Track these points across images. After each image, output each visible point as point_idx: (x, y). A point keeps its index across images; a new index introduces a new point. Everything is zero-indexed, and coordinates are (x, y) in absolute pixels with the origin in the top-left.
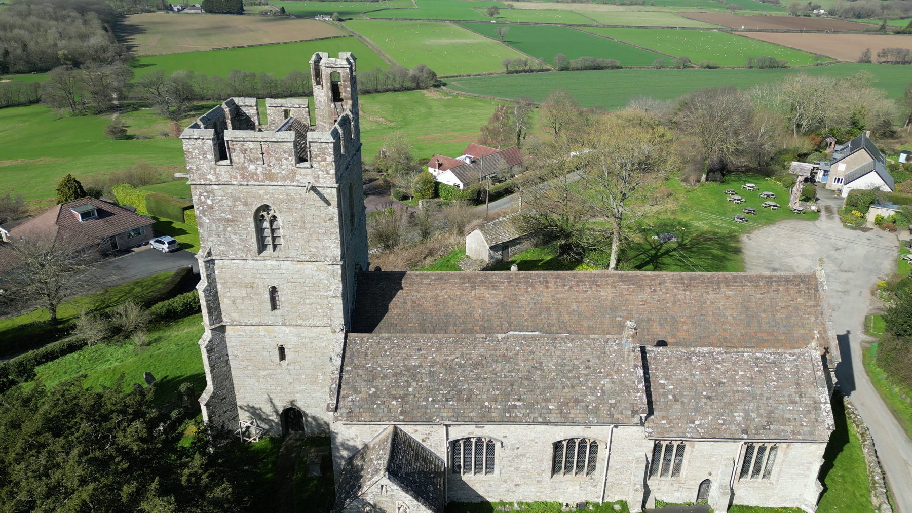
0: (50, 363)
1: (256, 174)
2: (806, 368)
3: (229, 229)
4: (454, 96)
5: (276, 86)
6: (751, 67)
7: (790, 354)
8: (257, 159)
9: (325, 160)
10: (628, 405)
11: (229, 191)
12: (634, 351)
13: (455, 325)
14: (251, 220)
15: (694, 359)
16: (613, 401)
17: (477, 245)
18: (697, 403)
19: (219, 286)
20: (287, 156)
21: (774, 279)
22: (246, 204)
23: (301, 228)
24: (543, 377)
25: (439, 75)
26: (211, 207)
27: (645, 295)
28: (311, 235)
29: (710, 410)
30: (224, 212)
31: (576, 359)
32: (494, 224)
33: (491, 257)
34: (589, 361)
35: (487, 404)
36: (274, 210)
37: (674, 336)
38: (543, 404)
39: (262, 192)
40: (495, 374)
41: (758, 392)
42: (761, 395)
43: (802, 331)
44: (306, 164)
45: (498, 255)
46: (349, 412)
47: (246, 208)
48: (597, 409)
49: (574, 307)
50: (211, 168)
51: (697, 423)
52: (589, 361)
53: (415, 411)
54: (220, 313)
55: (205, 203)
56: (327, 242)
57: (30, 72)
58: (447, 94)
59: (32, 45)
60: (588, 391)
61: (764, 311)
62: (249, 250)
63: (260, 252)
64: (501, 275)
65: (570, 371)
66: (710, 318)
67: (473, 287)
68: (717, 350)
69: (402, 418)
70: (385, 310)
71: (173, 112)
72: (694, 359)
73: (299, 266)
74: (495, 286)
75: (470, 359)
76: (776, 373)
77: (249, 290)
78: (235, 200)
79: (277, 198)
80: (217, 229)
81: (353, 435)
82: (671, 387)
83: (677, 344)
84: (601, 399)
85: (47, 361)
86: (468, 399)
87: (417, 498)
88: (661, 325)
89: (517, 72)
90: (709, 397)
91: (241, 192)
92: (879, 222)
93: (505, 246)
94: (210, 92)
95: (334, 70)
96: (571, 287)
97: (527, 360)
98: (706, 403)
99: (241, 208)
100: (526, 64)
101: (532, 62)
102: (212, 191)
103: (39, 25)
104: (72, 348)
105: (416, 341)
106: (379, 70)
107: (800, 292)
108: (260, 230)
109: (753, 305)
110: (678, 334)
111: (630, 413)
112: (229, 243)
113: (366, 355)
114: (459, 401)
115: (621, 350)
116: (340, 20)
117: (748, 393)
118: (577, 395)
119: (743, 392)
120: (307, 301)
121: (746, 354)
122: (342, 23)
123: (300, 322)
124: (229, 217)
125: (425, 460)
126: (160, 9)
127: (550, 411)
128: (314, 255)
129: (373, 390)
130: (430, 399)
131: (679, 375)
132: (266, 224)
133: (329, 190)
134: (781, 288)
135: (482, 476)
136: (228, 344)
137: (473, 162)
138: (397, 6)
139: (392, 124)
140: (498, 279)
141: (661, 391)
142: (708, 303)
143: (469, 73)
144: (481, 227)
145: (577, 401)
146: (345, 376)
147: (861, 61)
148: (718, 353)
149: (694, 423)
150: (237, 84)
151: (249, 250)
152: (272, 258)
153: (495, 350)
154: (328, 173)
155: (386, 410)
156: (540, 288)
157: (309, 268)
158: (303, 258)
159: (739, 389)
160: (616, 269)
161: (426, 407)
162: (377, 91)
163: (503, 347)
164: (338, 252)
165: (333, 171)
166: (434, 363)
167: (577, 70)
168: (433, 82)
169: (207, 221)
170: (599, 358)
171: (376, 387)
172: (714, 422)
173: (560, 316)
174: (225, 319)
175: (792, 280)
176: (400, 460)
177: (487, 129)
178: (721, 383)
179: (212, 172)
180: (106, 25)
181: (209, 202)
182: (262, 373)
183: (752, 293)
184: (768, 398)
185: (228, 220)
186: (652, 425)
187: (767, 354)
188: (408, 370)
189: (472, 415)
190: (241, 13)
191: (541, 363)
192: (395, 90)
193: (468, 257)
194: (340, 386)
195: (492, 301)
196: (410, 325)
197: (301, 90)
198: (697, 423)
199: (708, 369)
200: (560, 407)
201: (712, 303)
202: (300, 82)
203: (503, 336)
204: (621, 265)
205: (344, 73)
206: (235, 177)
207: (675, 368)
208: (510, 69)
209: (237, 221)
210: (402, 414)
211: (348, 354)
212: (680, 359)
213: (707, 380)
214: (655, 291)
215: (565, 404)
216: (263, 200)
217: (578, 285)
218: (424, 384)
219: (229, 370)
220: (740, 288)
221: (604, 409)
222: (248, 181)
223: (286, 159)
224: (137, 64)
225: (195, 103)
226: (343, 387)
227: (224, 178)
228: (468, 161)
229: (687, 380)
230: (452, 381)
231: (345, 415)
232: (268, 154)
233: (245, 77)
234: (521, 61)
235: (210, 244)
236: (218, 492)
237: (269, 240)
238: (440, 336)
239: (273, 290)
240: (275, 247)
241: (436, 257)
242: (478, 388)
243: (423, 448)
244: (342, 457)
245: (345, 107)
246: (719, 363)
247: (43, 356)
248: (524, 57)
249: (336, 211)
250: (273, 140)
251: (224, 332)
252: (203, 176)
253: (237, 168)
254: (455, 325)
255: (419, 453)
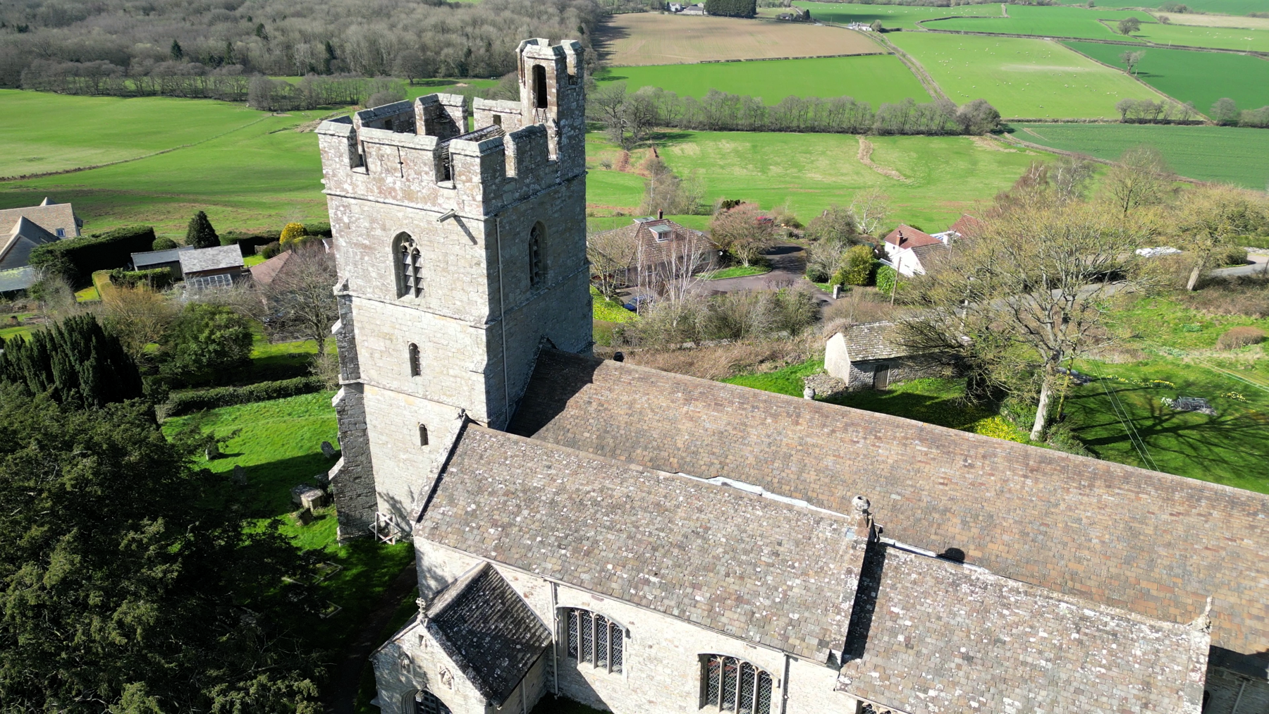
0: (281, 400)
1: (394, 189)
2: (1173, 660)
4: (1020, 150)
5: (763, 115)
7: (1152, 627)
8: (395, 169)
9: (470, 180)
10: (817, 629)
12: (854, 548)
13: (646, 448)
15: (965, 588)
16: (796, 616)
17: (837, 358)
18: (944, 661)
19: (356, 331)
21: (1207, 494)
22: (384, 229)
24: (703, 551)
25: (1004, 116)
27: (952, 470)
29: (963, 681)
30: (361, 235)
31: (761, 536)
32: (871, 329)
33: (854, 378)
34: (780, 544)
35: (610, 567)
36: (420, 242)
37: (979, 547)
38: (689, 590)
39: (400, 215)
40: (637, 528)
41: (1064, 676)
42: (1068, 682)
43: (1233, 599)
44: (449, 184)
45: (868, 377)
46: (434, 528)
48: (766, 621)
49: (829, 461)
50: (347, 175)
51: (932, 693)
52: (780, 544)
53: (513, 550)
54: (357, 367)
55: (341, 220)
56: (474, 296)
57: (489, 77)
58: (1009, 145)
59: (497, 46)
60: (762, 590)
61: (1169, 545)
63: (400, 295)
65: (746, 552)
66: (1057, 533)
67: (688, 401)
68: (1011, 583)
69: (494, 554)
70: (561, 407)
71: (627, 139)
72: (965, 588)
73: (441, 322)
74: (718, 405)
75: (611, 497)
76: (1111, 652)
77: (388, 342)
78: (373, 221)
81: (440, 561)
82: (908, 623)
83: (981, 562)
84: (778, 608)
85: (278, 397)
86: (588, 554)
87: (464, 668)
88: (964, 523)
89: (1141, 121)
90: (969, 659)
91: (378, 212)
93: (881, 366)
94: (679, 117)
95: (537, 62)
96: (833, 431)
97: (689, 519)
98: (959, 667)
99: (378, 232)
100: (1159, 109)
101: (1172, 107)
103: (512, 21)
104: (309, 389)
105: (550, 454)
106: (911, 103)
107: (1252, 527)
108: (400, 266)
109: (1149, 530)
110: (990, 545)
111: (816, 642)
112: (366, 276)
113: (481, 458)
114: (574, 549)
115: (837, 542)
116: (883, 31)
117: (1044, 672)
118: (743, 591)
119: (1034, 667)
120: (451, 372)
121: (1063, 605)
122: (885, 35)
123: (444, 398)
124: (367, 242)
125: (518, 623)
126: (654, 9)
127: (695, 604)
128: (458, 311)
129: (473, 506)
130: (539, 539)
131: (928, 606)
132: (409, 260)
133: (475, 223)
134: (1215, 513)
135: (602, 672)
136: (367, 410)
138: (975, 14)
139: (908, 181)
141: (889, 624)
142: (1062, 506)
143: (1056, 118)
144: (847, 329)
145: (739, 600)
146: (446, 478)
148: (1011, 590)
149: (925, 691)
150: (713, 109)
153: (649, 493)
155: (478, 538)
156: (785, 422)
157: (453, 326)
158: (445, 311)
159: (1030, 660)
160: (1044, 437)
161: (530, 548)
162: (903, 133)
163: (662, 491)
164: (485, 311)
165: (480, 198)
166: (561, 490)
167: (1253, 126)
168: (992, 126)
170: (797, 544)
171: (478, 506)
172: (962, 702)
173: (801, 471)
174: (364, 378)
175: (1243, 504)
176: (470, 610)
177: (1007, 197)
178: (997, 641)
180: (583, 25)
181: (346, 220)
182: (402, 456)
183: (1155, 509)
184: (1078, 691)
185: (365, 247)
186: (853, 672)
187: (1108, 617)
188: (525, 492)
189: (584, 576)
190: (752, 17)
191: (707, 529)
192: (930, 133)
193: (825, 372)
194: (434, 491)
195: (708, 425)
196: (587, 435)
197: (795, 124)
198: (932, 693)
199: (983, 611)
200: (711, 602)
201: (1069, 508)
202: (795, 112)
203: (668, 475)
204: (1054, 429)
205: (550, 67)
206: (372, 191)
207: (926, 594)
208: (1129, 116)
210: (496, 549)
211: (459, 450)
212: (938, 581)
213: (975, 630)
214: (971, 466)
215: (722, 600)
216: (401, 225)
217: (845, 429)
218: (538, 516)
219: (367, 442)
220: (1132, 496)
221: (777, 624)
224: (606, 76)
225: (657, 130)
226: (439, 492)
227: (361, 191)
229: (939, 618)
230: (576, 521)
231: (427, 530)
233: (726, 99)
234: (1151, 104)
235: (347, 275)
236: (158, 572)
237: (411, 282)
238: (582, 454)
239: (414, 350)
240: (418, 291)
241: (780, 363)
242: (606, 541)
243: (524, 606)
244: (429, 587)
246: (1007, 606)
247: (275, 391)
248: (1157, 97)
249: (483, 253)
251: (362, 392)
252: (339, 184)
255: (514, 610)
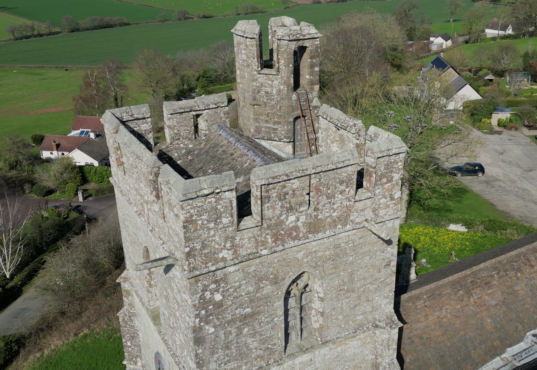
1: (296, 228)
3: (246, 330)
6: (239, 14)
8: (301, 204)
9: (390, 180)
11: (253, 268)
14: (281, 303)
20: (343, 188)
22: (276, 281)
23: (348, 291)
26: (219, 305)
28: (359, 298)
30: (241, 306)
39: (300, 255)
47: (274, 288)
50: (226, 239)
55: (211, 300)
62: (272, 352)
64: (486, 269)
79: (321, 257)
80: (226, 337)
91: (270, 265)
92: (500, 124)
95: (300, 43)
99: (268, 289)
102: (225, 279)
124: (248, 310)
132: (292, 302)
133: (390, 224)
137: (97, 136)
140: (486, 273)
147: (314, 3)
151: (272, 352)
152: (304, 350)
154: (392, 198)
169: (212, 330)
179: (228, 245)
181: (218, 297)
185: (246, 316)
206: (264, 244)
209: (259, 313)
222: (284, 242)
223: (341, 193)
227: (243, 252)
228: (92, 135)
232: (318, 190)
245: (310, 96)
250: (331, 167)
253: (269, 227)
254: (475, 349)
